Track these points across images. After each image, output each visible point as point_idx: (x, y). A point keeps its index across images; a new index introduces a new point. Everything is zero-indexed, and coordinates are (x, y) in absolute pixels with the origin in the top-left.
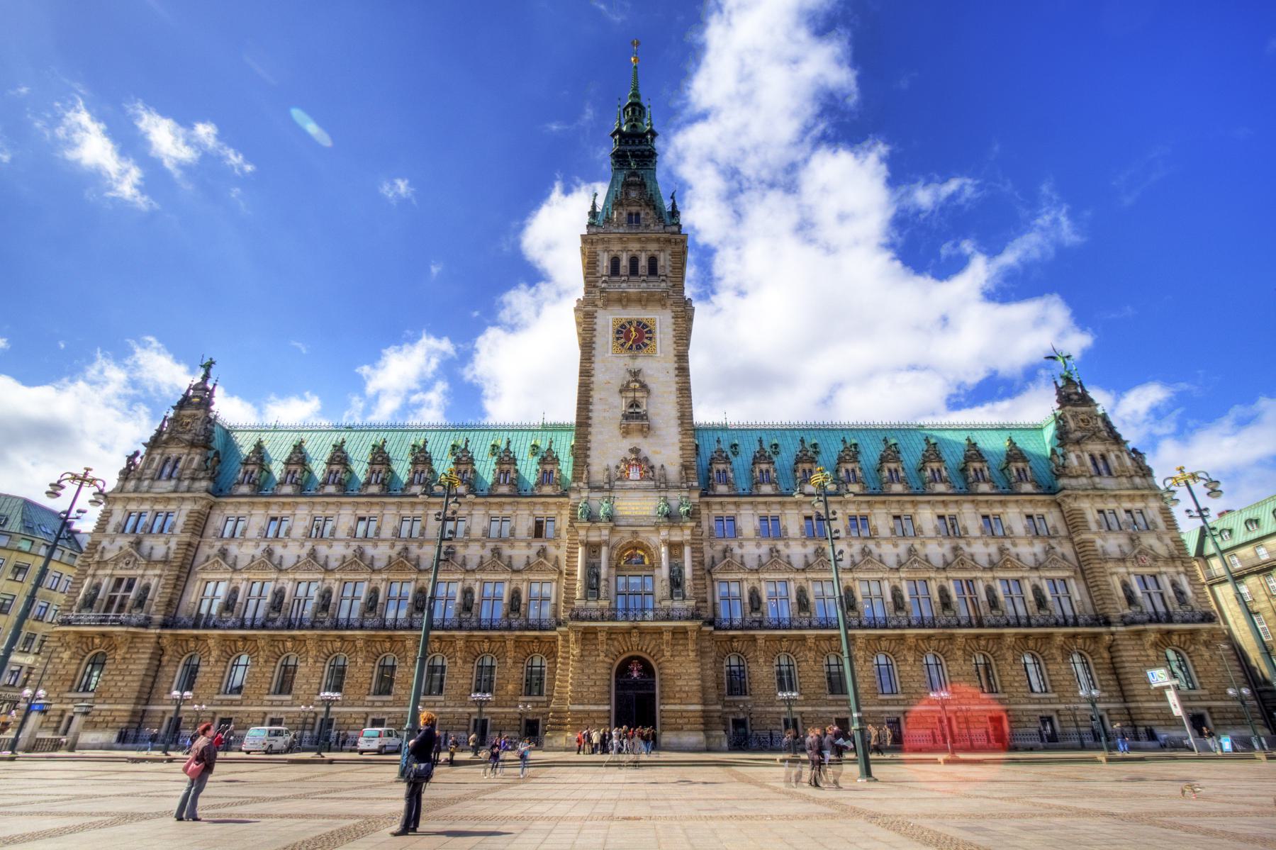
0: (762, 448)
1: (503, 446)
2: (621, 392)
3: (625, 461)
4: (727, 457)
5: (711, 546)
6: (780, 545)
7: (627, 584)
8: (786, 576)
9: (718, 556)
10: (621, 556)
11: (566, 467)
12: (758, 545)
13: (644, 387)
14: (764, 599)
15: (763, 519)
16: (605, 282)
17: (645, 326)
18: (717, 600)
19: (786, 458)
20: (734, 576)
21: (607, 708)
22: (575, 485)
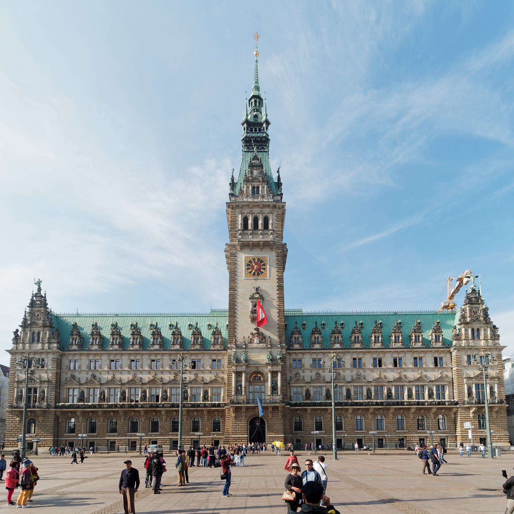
0: (316, 326)
1: (195, 325)
2: (250, 299)
3: (252, 334)
4: (300, 331)
5: (291, 372)
6: (321, 372)
7: (254, 388)
8: (322, 384)
9: (293, 376)
10: (251, 377)
11: (225, 334)
12: (311, 371)
13: (262, 297)
14: (312, 394)
15: (314, 360)
16: (240, 234)
17: (262, 261)
18: (292, 395)
19: (328, 331)
20: (300, 385)
21: (247, 436)
22: (229, 346)
